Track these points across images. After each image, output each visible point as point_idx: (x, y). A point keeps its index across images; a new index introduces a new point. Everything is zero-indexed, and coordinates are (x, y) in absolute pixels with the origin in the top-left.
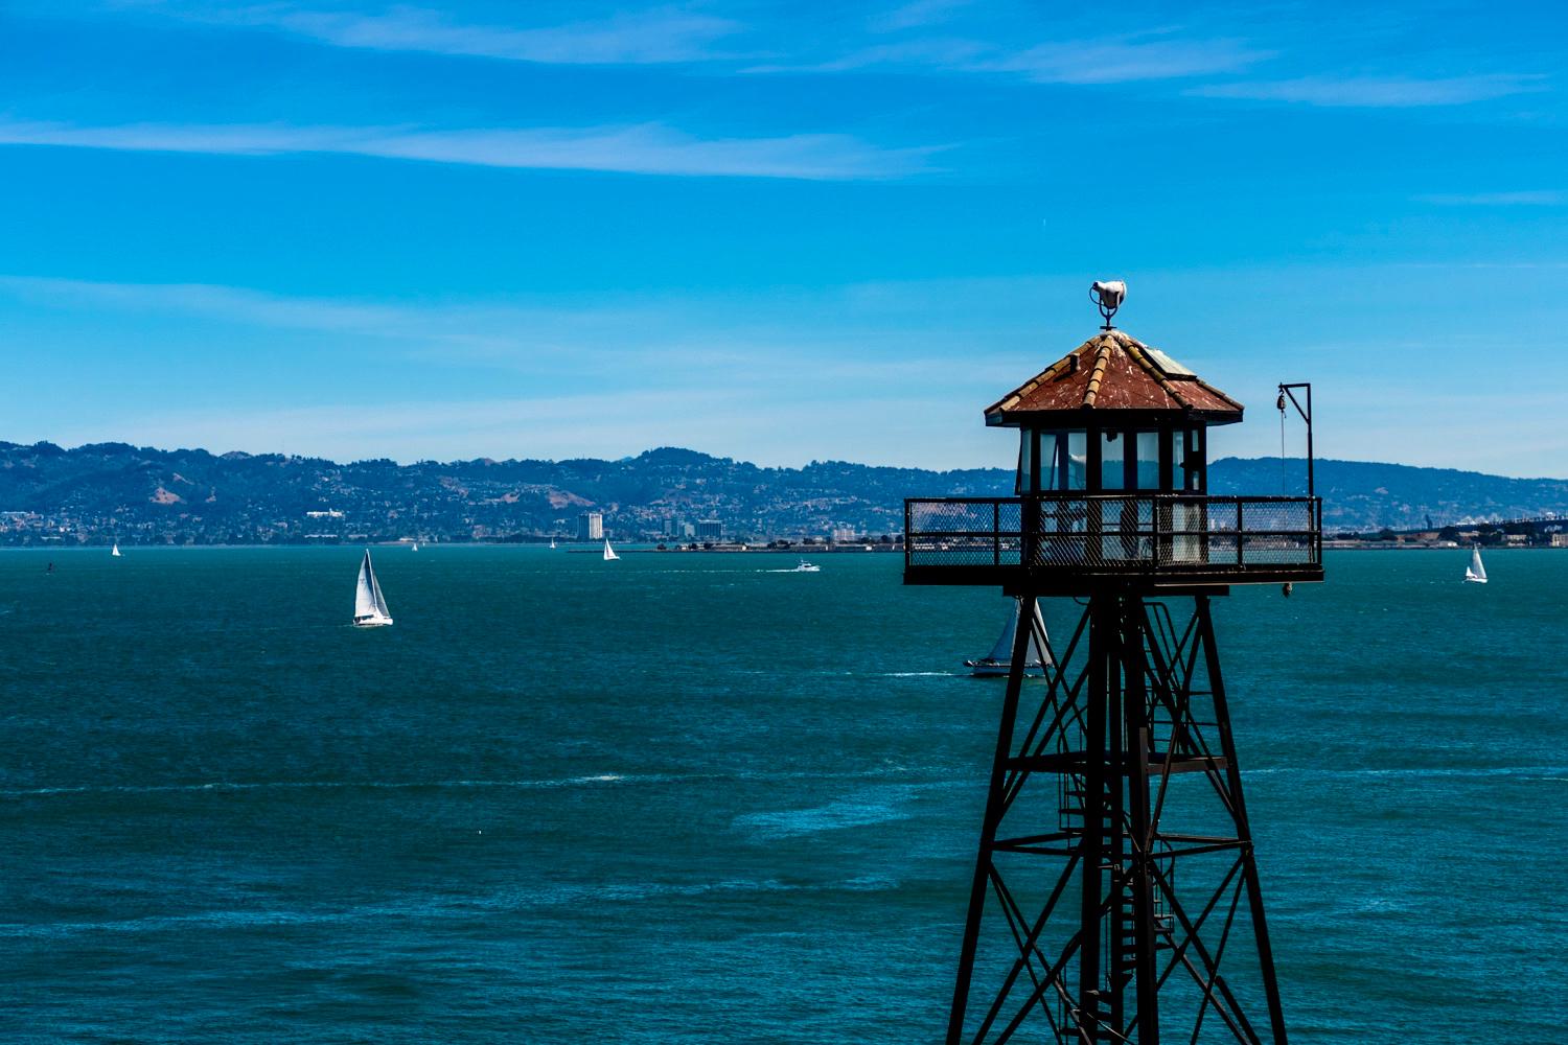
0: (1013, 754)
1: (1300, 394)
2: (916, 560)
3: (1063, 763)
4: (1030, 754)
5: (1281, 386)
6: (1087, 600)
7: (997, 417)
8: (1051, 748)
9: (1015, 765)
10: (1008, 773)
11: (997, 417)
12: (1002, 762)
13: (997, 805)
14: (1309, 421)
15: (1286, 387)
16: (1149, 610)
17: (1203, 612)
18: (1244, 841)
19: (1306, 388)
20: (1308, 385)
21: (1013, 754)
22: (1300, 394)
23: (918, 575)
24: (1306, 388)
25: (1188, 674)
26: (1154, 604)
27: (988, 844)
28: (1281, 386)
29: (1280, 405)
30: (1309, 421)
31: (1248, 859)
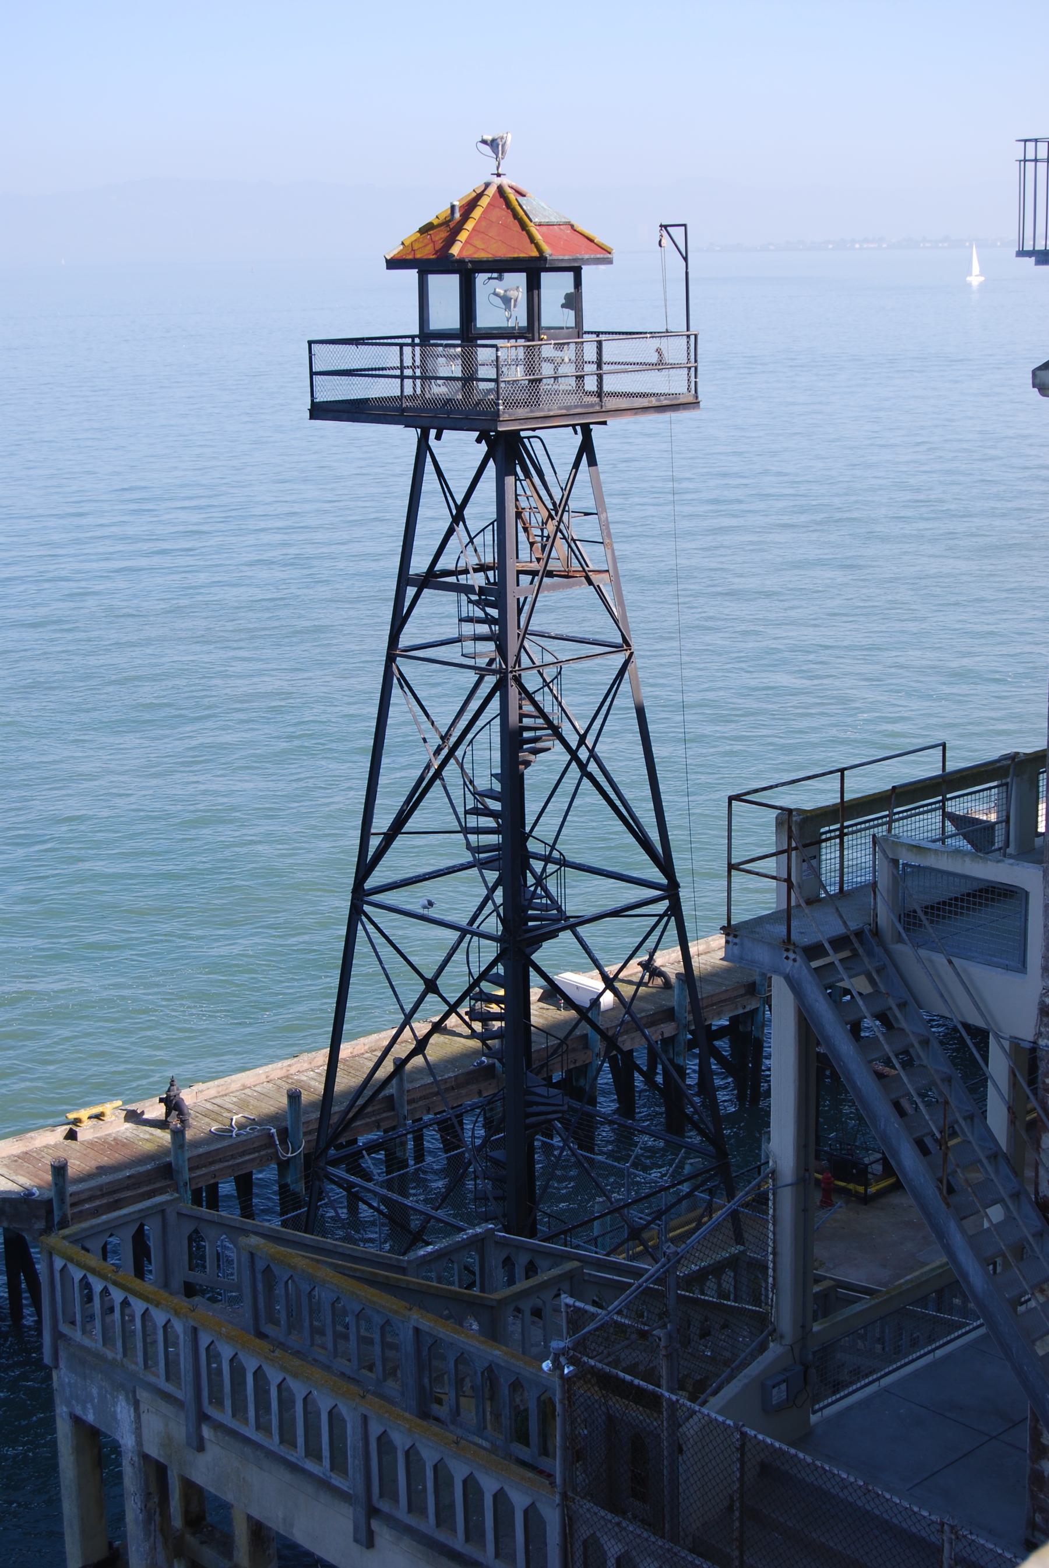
1: (678, 233)
2: (320, 398)
5: (661, 226)
10: (411, 591)
12: (404, 578)
14: (686, 259)
15: (666, 227)
16: (526, 441)
19: (683, 228)
20: (685, 225)
21: (419, 564)
22: (678, 233)
23: (320, 411)
24: (683, 228)
26: (528, 438)
28: (661, 226)
29: (660, 245)
30: (686, 259)
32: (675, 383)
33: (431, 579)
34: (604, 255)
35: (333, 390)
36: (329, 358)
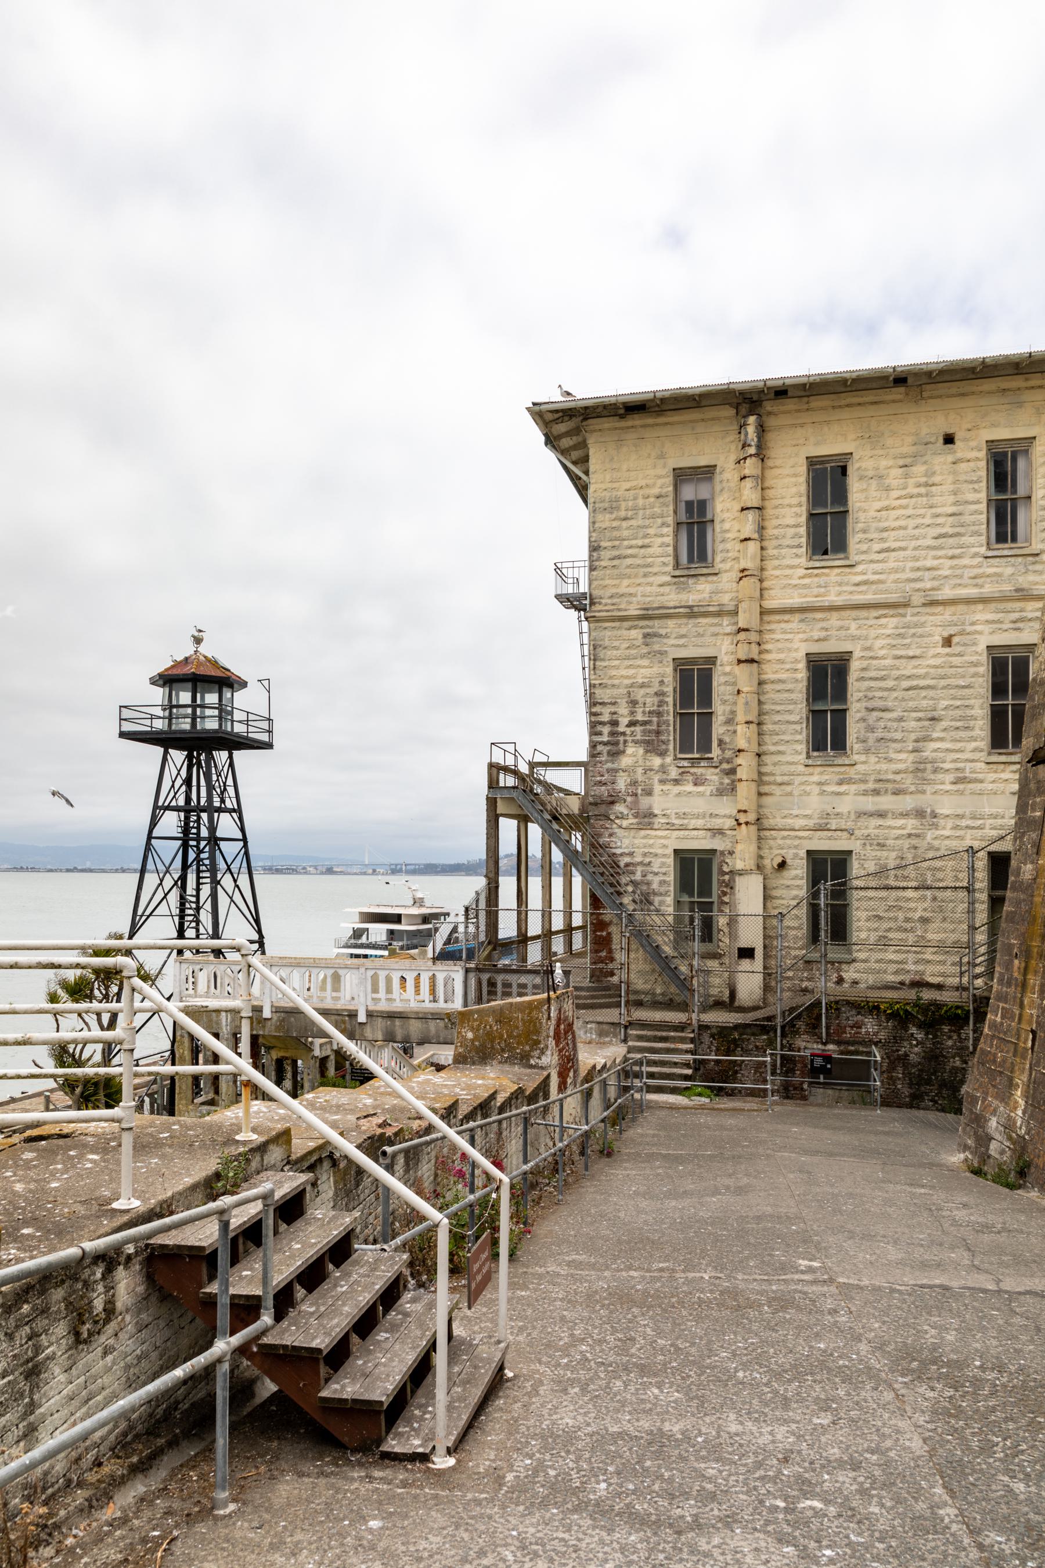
0: (160, 804)
3: (177, 809)
4: (166, 804)
6: (186, 753)
7: (153, 682)
8: (174, 803)
9: (161, 808)
11: (153, 682)
12: (156, 807)
13: (154, 823)
17: (231, 757)
18: (244, 839)
23: (123, 735)
25: (226, 778)
27: (150, 837)
31: (245, 846)
32: (264, 737)
33: (168, 808)
34: (244, 684)
35: (127, 727)
36: (126, 714)
